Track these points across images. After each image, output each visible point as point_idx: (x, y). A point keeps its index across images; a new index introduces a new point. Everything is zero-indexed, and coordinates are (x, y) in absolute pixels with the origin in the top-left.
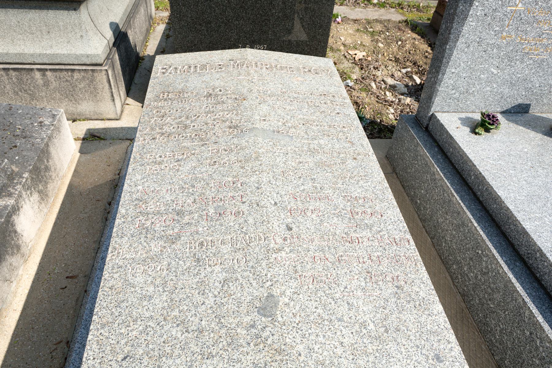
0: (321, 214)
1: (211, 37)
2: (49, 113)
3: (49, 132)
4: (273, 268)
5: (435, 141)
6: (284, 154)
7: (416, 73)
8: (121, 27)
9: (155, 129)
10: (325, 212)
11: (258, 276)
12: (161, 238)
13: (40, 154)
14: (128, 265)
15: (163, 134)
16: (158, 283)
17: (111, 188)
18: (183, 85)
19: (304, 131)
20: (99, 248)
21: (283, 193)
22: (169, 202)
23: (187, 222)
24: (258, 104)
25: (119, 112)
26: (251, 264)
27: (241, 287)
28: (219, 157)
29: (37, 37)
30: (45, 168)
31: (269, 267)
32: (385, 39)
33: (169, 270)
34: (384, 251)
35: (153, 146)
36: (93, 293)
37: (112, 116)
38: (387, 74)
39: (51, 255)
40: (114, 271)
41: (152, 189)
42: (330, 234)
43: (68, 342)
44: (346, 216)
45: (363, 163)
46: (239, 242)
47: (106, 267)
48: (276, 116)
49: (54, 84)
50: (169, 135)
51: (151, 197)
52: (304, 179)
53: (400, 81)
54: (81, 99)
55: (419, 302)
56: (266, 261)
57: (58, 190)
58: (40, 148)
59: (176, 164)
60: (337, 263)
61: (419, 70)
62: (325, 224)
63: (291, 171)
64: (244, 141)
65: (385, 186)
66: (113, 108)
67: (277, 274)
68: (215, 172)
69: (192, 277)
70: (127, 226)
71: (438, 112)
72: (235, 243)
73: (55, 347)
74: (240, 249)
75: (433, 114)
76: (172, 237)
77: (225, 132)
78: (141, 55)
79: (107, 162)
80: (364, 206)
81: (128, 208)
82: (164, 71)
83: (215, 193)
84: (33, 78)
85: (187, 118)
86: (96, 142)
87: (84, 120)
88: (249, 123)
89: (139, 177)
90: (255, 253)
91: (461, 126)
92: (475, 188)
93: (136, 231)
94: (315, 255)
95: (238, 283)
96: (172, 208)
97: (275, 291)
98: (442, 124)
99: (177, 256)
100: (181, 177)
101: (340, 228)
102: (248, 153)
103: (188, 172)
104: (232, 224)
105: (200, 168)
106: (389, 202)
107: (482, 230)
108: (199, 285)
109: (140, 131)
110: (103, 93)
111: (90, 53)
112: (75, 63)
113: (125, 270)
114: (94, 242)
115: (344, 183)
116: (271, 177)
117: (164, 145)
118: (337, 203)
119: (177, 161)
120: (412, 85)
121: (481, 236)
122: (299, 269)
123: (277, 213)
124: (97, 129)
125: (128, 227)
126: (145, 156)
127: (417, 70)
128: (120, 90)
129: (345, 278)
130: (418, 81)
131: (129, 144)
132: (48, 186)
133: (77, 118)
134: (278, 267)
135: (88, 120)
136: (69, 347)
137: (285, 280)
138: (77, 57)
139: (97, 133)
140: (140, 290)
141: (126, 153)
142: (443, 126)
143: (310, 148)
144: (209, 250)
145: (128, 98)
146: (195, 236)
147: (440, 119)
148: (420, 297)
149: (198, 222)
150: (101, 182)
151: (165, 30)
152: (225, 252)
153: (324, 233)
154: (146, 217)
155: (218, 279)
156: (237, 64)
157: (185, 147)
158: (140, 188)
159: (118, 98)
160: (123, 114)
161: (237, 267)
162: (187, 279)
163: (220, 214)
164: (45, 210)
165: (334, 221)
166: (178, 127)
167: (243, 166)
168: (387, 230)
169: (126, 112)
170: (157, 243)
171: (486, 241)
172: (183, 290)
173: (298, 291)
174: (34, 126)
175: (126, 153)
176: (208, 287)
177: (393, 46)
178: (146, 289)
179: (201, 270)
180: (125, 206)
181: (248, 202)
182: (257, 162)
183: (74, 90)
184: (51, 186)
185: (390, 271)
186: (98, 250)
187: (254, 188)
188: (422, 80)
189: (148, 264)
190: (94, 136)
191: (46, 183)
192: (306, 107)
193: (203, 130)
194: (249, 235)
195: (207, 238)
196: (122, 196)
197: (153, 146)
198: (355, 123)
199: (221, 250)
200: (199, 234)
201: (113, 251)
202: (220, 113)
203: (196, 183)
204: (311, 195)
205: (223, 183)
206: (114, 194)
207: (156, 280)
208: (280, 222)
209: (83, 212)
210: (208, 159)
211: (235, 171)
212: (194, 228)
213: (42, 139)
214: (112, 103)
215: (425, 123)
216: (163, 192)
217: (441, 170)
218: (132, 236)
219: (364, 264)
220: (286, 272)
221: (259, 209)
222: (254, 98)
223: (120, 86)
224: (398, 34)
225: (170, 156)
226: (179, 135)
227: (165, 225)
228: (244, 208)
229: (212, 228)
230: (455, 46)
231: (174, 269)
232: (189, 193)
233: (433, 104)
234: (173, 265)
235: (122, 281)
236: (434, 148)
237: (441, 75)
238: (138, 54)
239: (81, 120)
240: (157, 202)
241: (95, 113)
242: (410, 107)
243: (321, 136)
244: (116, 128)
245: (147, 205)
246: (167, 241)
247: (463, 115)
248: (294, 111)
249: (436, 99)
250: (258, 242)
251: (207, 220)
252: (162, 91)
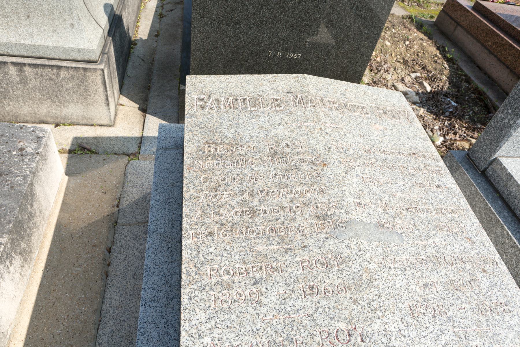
1: (238, 40)
2: (32, 135)
3: (34, 165)
5: (496, 190)
7: (426, 79)
8: (115, 9)
9: (209, 213)
13: (22, 202)
15: (222, 225)
17: (110, 227)
18: (233, 131)
20: (100, 321)
24: (344, 174)
25: (112, 117)
28: (316, 278)
29: (13, 21)
30: (28, 217)
32: (391, 36)
35: (212, 249)
37: (105, 122)
38: (396, 78)
39: (37, 336)
48: (371, 196)
49: (33, 82)
50: (232, 226)
54: (68, 101)
57: (44, 238)
58: (21, 192)
59: (254, 290)
61: (428, 75)
71: (503, 156)
75: (496, 159)
77: (312, 225)
78: (133, 39)
79: (102, 187)
82: (201, 103)
84: (6, 73)
85: (252, 195)
86: (86, 157)
87: (69, 125)
88: (343, 211)
89: (202, 317)
98: (510, 174)
100: (268, 318)
102: (356, 270)
109: (187, 216)
110: (96, 96)
111: (82, 47)
112: (62, 58)
114: (94, 311)
115: (489, 323)
117: (228, 248)
119: (255, 284)
120: (422, 93)
124: (86, 138)
126: (203, 270)
127: (426, 75)
128: (114, 89)
130: (429, 89)
131: (127, 162)
132: (32, 238)
133: (60, 122)
135: (74, 125)
138: (65, 50)
139: (86, 143)
141: (125, 174)
142: (512, 177)
143: (428, 254)
145: (121, 96)
147: (506, 167)
151: (157, 8)
156: (298, 99)
159: (113, 100)
160: (117, 118)
166: (242, 212)
167: (355, 297)
169: (120, 115)
174: (11, 156)
175: (125, 174)
177: (401, 46)
182: (373, 290)
183: (59, 90)
184: (35, 236)
186: (99, 325)
188: (432, 87)
190: (82, 148)
191: (30, 236)
192: (401, 177)
193: (279, 221)
197: (212, 249)
198: (462, 203)
202: (297, 189)
203: (294, 332)
205: (335, 335)
206: (114, 235)
209: (76, 265)
210: (300, 280)
211: (345, 309)
213: (25, 177)
214: (105, 108)
215: (483, 166)
223: (114, 84)
224: (404, 32)
225: (242, 271)
226: (247, 229)
233: (500, 148)
236: (498, 201)
238: (130, 38)
239: (66, 124)
241: (84, 117)
242: (423, 119)
243: (433, 230)
244: (110, 138)
248: (389, 186)
249: (505, 144)
252: (205, 141)
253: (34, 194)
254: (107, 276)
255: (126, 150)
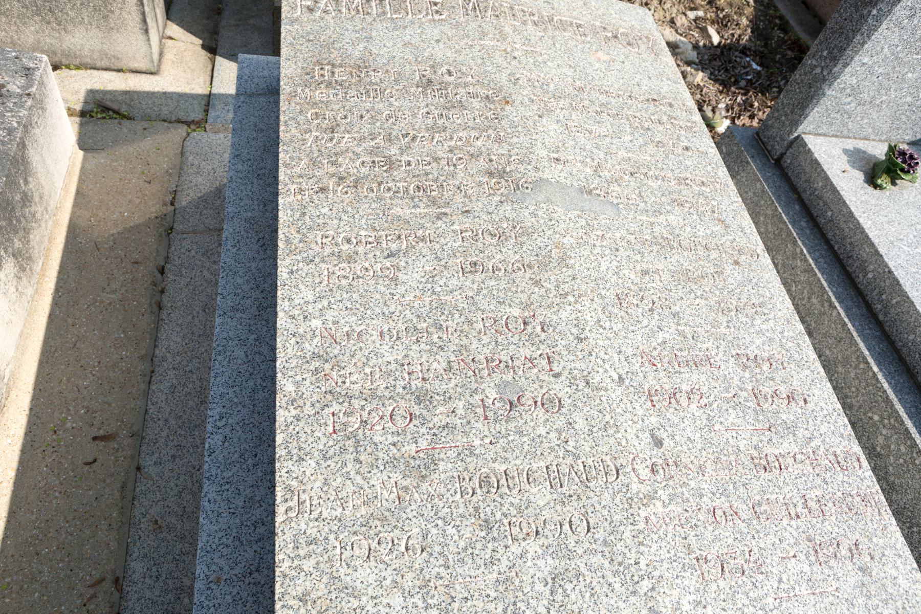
0: (706, 401)
2: (15, 64)
3: (23, 113)
4: (647, 546)
5: (794, 189)
6: (611, 249)
7: (713, 22)
9: (320, 162)
10: (712, 398)
11: (620, 564)
12: (393, 463)
13: (9, 170)
14: (332, 537)
15: (341, 178)
16: (410, 584)
17: (161, 236)
18: (361, 47)
19: (637, 192)
20: (153, 372)
21: (630, 351)
22: (393, 366)
23: (444, 423)
24: (537, 117)
25: (156, 57)
26: (600, 535)
27: (592, 595)
28: (481, 252)
30: (22, 198)
31: (641, 544)
33: (428, 549)
34: (825, 487)
35: (325, 210)
36: (204, 539)
37: (142, 66)
38: (662, 18)
39: (52, 388)
40: (302, 552)
41: (345, 329)
42: (730, 449)
43: (117, 581)
44: (748, 404)
45: (752, 274)
46: (566, 478)
47: (279, 542)
48: (577, 151)
50: (356, 182)
51: (348, 351)
52: (659, 315)
53: (685, 36)
54: (72, 21)
55: (901, 601)
56: (630, 527)
57: (50, 242)
58: (7, 154)
59: (388, 264)
60: (755, 522)
61: (718, 16)
62: (717, 427)
63: (632, 293)
64: (526, 213)
65: (799, 328)
66: (144, 48)
67: (657, 559)
68: (479, 291)
69: (482, 569)
70: (306, 429)
71: (809, 133)
72: (557, 480)
73: (91, 591)
74: (570, 496)
75: (798, 136)
76: (418, 462)
77: (480, 184)
79: (143, 173)
80: (773, 379)
81: (299, 378)
83: (491, 347)
85: (390, 140)
86: (113, 124)
87: (78, 68)
88: (529, 167)
89: (310, 296)
90: (604, 507)
91: (849, 168)
92: (873, 296)
93: (331, 443)
94: (714, 504)
95: (582, 583)
96: (402, 383)
97: (661, 604)
98: (816, 160)
99: (440, 514)
100: (407, 299)
101: (743, 436)
102: (542, 245)
103: (421, 287)
104: (542, 431)
105: (444, 280)
106: (812, 368)
107: (886, 379)
108: (501, 588)
109: (286, 165)
110: (124, 13)
113: (326, 550)
114: (142, 358)
115: (730, 324)
116: (600, 309)
117: (350, 209)
118: (727, 373)
119: (389, 256)
120: (705, 45)
121: (886, 391)
122: (694, 541)
123: (629, 405)
125: (309, 432)
126: (311, 236)
127: (713, 15)
128: (156, 6)
129: (774, 557)
130: (716, 39)
131: (185, 134)
132: (31, 236)
133: (61, 62)
134: (656, 542)
135: (86, 68)
136: (120, 590)
137: (675, 573)
139: (111, 101)
140: (371, 603)
141: (182, 154)
142: (819, 164)
143: (655, 234)
144: (506, 497)
145: (169, 23)
146: (468, 460)
147: (813, 150)
148: (902, 591)
149: (469, 423)
150: (137, 219)
152: (541, 503)
153: (719, 450)
154: (346, 404)
155: (539, 574)
156: (471, 4)
157: (399, 218)
158: (316, 323)
159: (154, 24)
160: (164, 60)
161: (573, 544)
162: (473, 574)
163: (511, 403)
164: (30, 291)
165: (731, 419)
166: (373, 162)
167: (538, 278)
168: (821, 435)
169: (169, 56)
170: (386, 478)
171: (895, 403)
172: (469, 603)
173: (702, 599)
175: (182, 154)
176: (521, 594)
178: (385, 601)
179: (500, 551)
180: (290, 373)
181: (565, 373)
182: (564, 270)
184: (35, 236)
185: (843, 532)
186: (151, 377)
187: (571, 338)
188: (722, 37)
189: (377, 535)
190: (105, 109)
191: (27, 231)
192: (628, 130)
193: (430, 176)
194: (584, 459)
195: (496, 465)
196: (279, 345)
197: (325, 210)
198: (720, 174)
199: (532, 498)
200: (477, 456)
201: (288, 496)
202: (461, 134)
203: (444, 317)
204: (678, 354)
205: (503, 322)
206: (169, 248)
207: (402, 576)
208: (639, 426)
209: (108, 290)
210: (458, 254)
211: (522, 292)
212: (462, 440)
214: (142, 37)
215: (778, 150)
216: (374, 338)
218: (325, 458)
219: (799, 520)
220: (672, 552)
221: (591, 394)
222: (526, 100)
225: (370, 240)
226: (380, 185)
227: (394, 429)
228: (560, 389)
229: (501, 441)
230: (890, 12)
231: (437, 549)
232: (433, 344)
233: (805, 118)
234: (434, 537)
235: (325, 579)
236: (794, 204)
237: (839, 66)
239: (72, 66)
240: (365, 365)
241: (104, 54)
242: (702, 91)
243: (669, 204)
244: (153, 93)
245: (342, 372)
246: (407, 473)
247: (850, 144)
248: (608, 140)
249: (814, 111)
250: (605, 479)
251: (486, 418)
252: (314, 60)
254: (160, 308)
255: (182, 115)
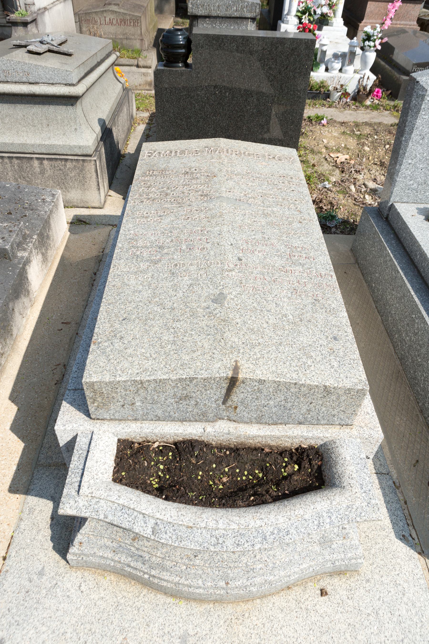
1: (190, 131)
3: (51, 207)
5: (392, 229)
8: (107, 124)
12: (148, 261)
15: (149, 199)
21: (239, 239)
25: (103, 201)
29: (38, 129)
32: (372, 142)
37: (97, 205)
43: (65, 365)
48: (240, 189)
49: (49, 173)
53: (382, 185)
62: (267, 260)
66: (98, 197)
71: (398, 202)
73: (55, 367)
75: (392, 204)
77: (197, 198)
78: (122, 152)
82: (150, 154)
84: (32, 166)
86: (83, 226)
87: (71, 207)
89: (132, 226)
91: (417, 214)
92: (419, 266)
104: (198, 255)
111: (82, 144)
112: (68, 153)
114: (83, 300)
124: (83, 215)
136: (66, 368)
138: (71, 147)
141: (109, 235)
150: (87, 257)
151: (145, 130)
158: (132, 232)
164: (45, 271)
169: (108, 202)
174: (38, 202)
175: (109, 235)
177: (380, 150)
183: (65, 178)
191: (47, 249)
213: (46, 212)
214: (97, 192)
217: (392, 252)
223: (104, 177)
224: (388, 137)
228: (209, 246)
230: (410, 137)
237: (398, 166)
238: (119, 151)
241: (82, 201)
247: (422, 206)
253: (48, 237)
254: (93, 286)
255: (111, 223)
